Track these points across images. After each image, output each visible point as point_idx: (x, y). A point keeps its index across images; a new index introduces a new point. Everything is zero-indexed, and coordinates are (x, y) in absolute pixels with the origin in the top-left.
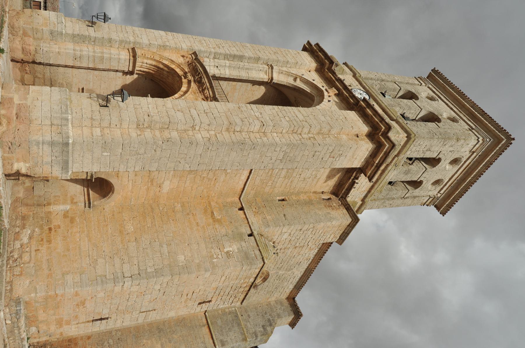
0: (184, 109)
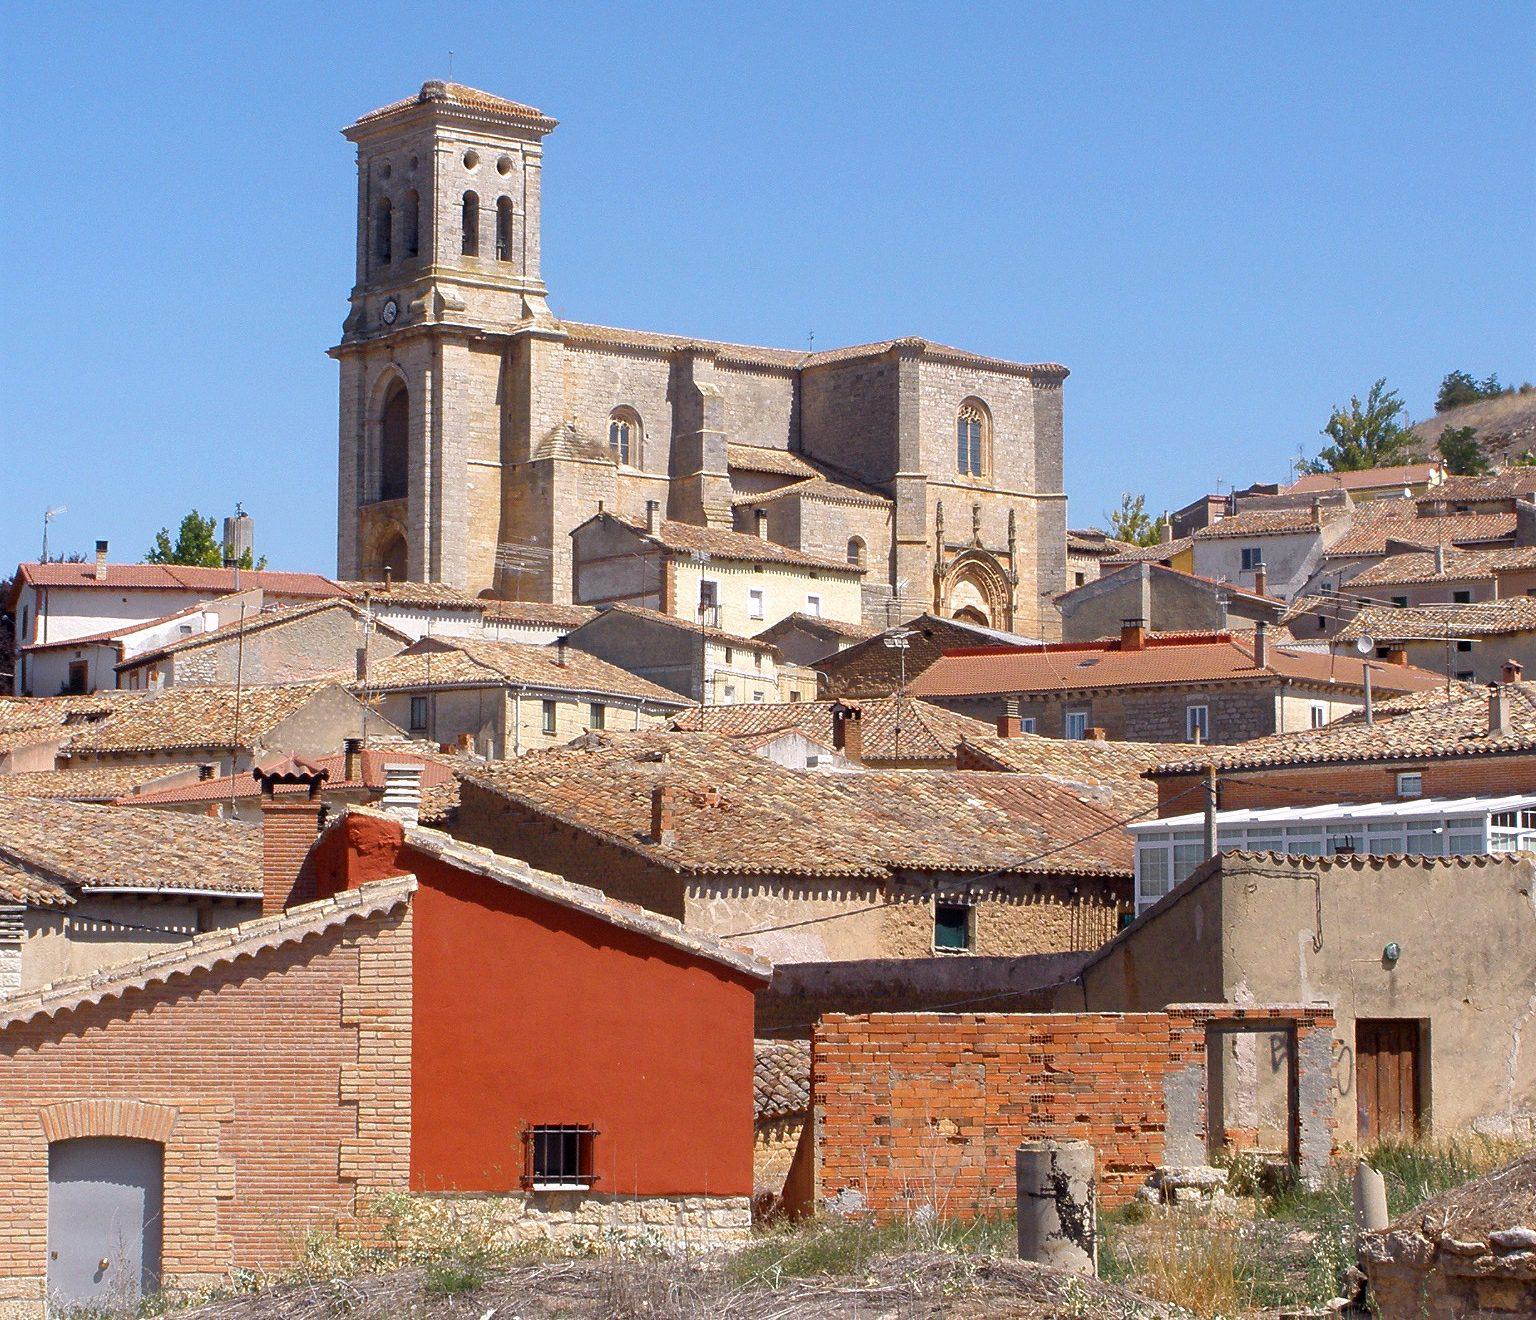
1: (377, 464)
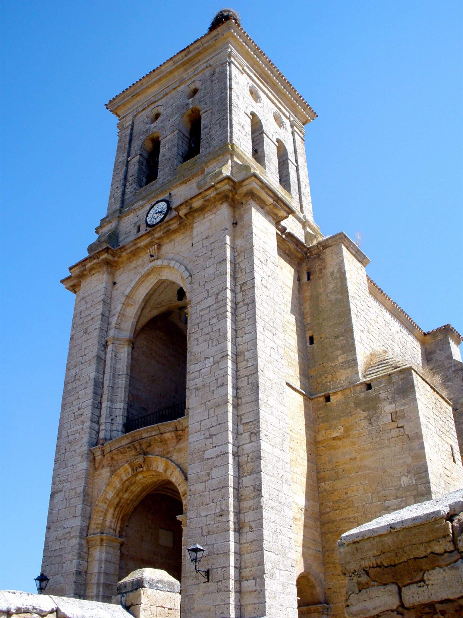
0: (205, 467)
1: (121, 394)
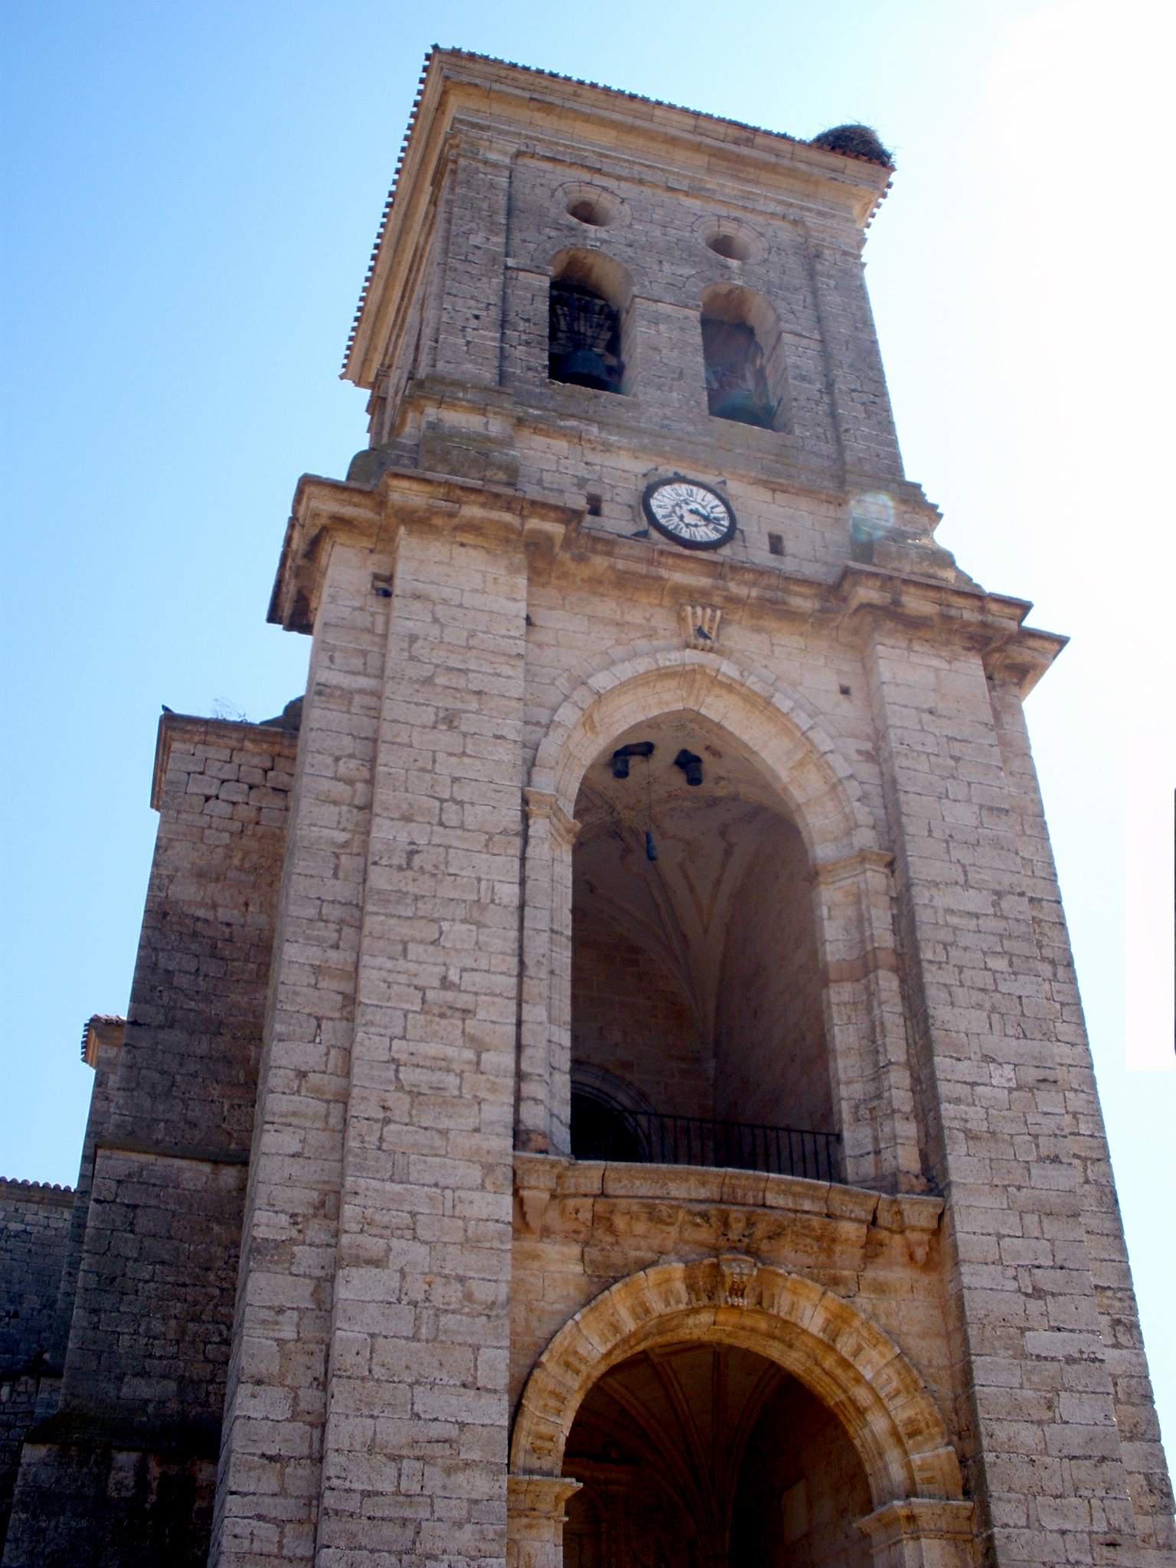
0: (1035, 1379)
